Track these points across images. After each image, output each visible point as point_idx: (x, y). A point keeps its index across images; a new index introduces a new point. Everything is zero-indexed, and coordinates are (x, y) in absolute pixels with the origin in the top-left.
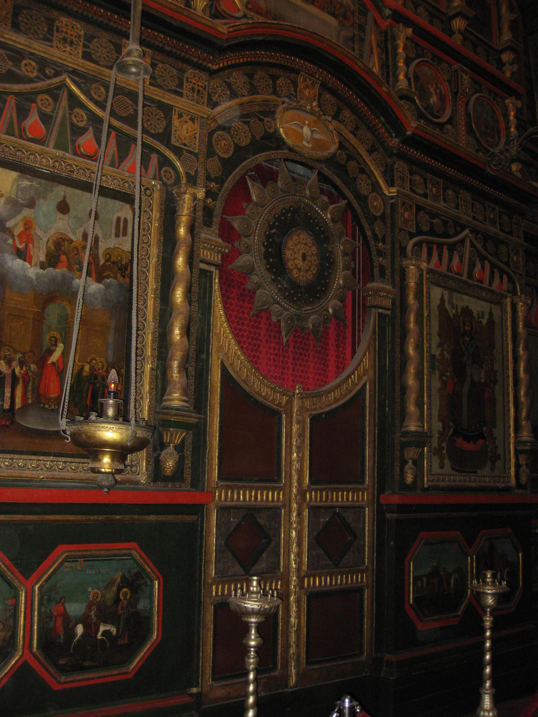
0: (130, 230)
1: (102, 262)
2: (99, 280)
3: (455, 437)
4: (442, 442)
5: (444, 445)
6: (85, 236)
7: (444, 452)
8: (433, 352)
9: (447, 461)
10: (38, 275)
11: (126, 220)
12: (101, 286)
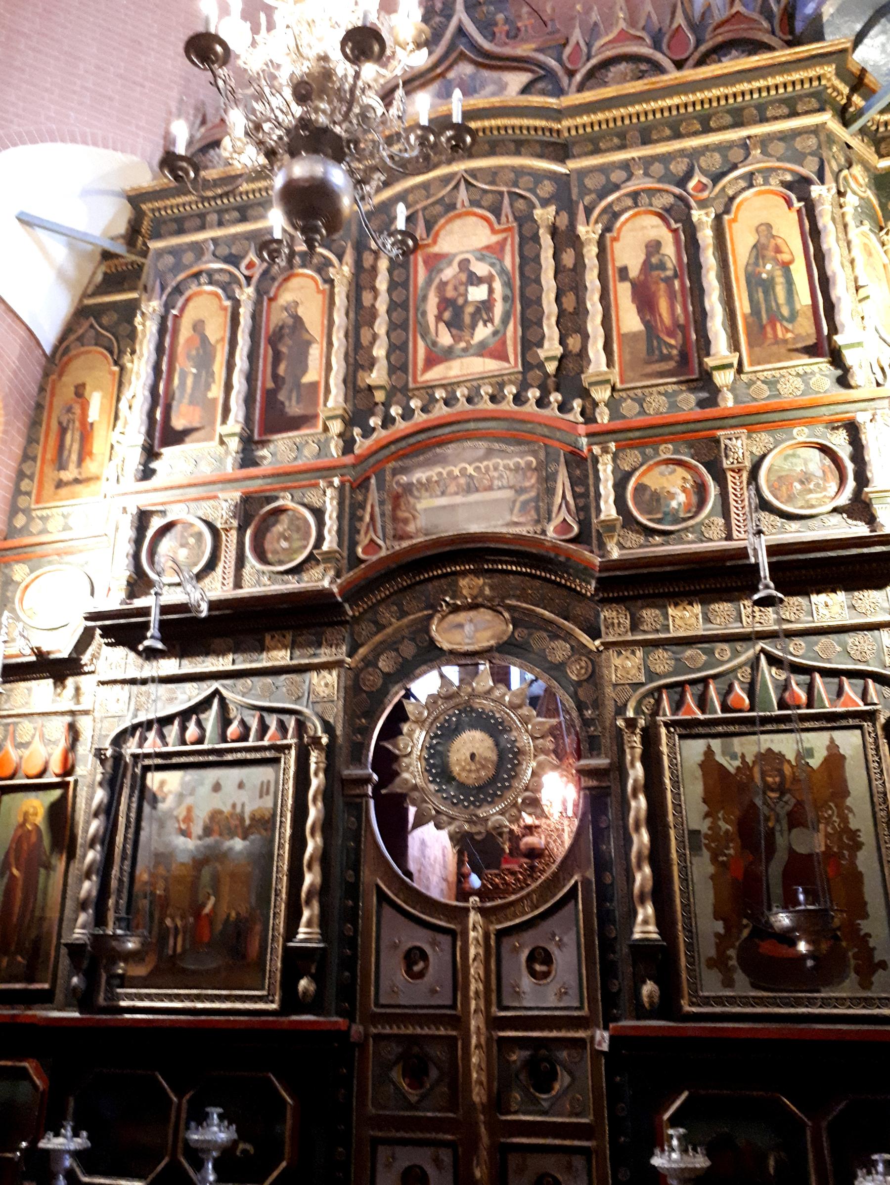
0: (272, 789)
1: (247, 822)
2: (244, 838)
3: (757, 940)
4: (728, 948)
5: (732, 952)
6: (234, 806)
7: (733, 962)
8: (694, 826)
9: (740, 977)
10: (197, 847)
11: (269, 782)
12: (247, 843)
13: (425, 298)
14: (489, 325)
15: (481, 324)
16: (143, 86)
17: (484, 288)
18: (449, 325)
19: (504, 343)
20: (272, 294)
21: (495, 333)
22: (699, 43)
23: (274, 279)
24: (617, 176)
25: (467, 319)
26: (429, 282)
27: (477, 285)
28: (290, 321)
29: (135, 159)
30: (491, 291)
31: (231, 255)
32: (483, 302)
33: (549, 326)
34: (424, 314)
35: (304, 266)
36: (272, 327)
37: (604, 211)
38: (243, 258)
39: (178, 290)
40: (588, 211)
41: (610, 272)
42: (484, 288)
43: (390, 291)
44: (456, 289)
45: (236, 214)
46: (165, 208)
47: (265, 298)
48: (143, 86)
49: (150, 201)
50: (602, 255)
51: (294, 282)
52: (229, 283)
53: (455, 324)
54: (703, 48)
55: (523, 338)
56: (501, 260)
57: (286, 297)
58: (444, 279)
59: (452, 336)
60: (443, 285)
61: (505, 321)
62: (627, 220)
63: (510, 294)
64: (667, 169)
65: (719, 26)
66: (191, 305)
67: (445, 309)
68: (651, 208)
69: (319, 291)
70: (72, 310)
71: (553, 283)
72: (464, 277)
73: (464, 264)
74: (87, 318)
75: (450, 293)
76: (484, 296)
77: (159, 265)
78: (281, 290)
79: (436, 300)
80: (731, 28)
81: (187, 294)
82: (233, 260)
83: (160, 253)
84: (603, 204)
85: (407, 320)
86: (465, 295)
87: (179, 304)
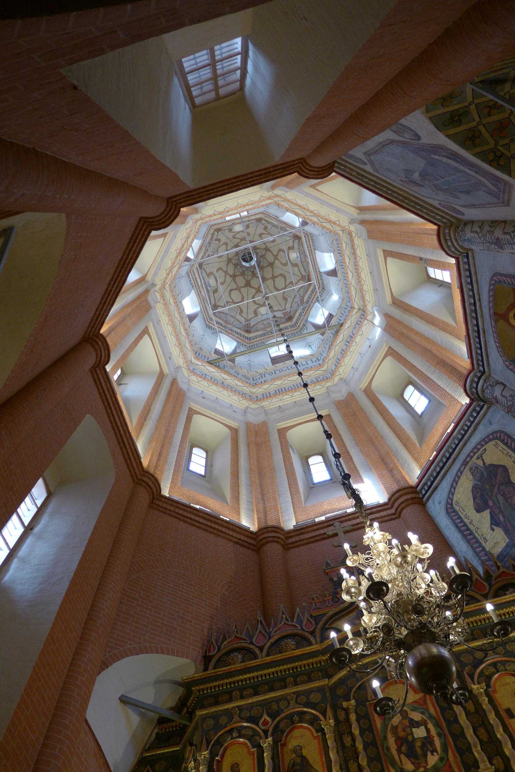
13: (385, 738)
14: (435, 753)
15: (429, 754)
16: (191, 622)
17: (423, 728)
18: (408, 756)
19: (450, 766)
20: (283, 742)
21: (441, 759)
22: (491, 586)
23: (283, 732)
24: (479, 655)
25: (419, 751)
26: (385, 727)
27: (418, 727)
28: (299, 760)
29: (188, 661)
30: (428, 731)
31: (250, 716)
32: (425, 738)
33: (477, 751)
34: (388, 749)
35: (301, 721)
36: (286, 764)
37: (480, 675)
38: (260, 718)
39: (219, 743)
40: (472, 677)
41: (502, 713)
42: (423, 728)
43: (362, 733)
44: (404, 731)
45: (251, 691)
46: (207, 689)
47: (279, 744)
48: (191, 622)
49: (198, 685)
50: (491, 701)
51: (297, 733)
52: (253, 736)
53: (411, 754)
54: (494, 588)
55: (463, 762)
56: (427, 710)
57: (292, 744)
58: (394, 725)
59: (412, 763)
60: (395, 729)
61: (445, 749)
62: (496, 679)
63: (442, 732)
64: (505, 649)
65: (497, 578)
66: (228, 752)
67: (402, 745)
68: (507, 672)
69: (315, 738)
70: (136, 761)
71: (467, 722)
72: (407, 723)
73: (404, 714)
74: (146, 766)
75: (402, 734)
76: (425, 735)
77: (204, 726)
78: (289, 738)
79: (394, 739)
80: (504, 578)
81: (226, 745)
82: (254, 720)
83: (204, 718)
84: (478, 671)
85: (378, 753)
86: (412, 733)
87: (220, 753)
